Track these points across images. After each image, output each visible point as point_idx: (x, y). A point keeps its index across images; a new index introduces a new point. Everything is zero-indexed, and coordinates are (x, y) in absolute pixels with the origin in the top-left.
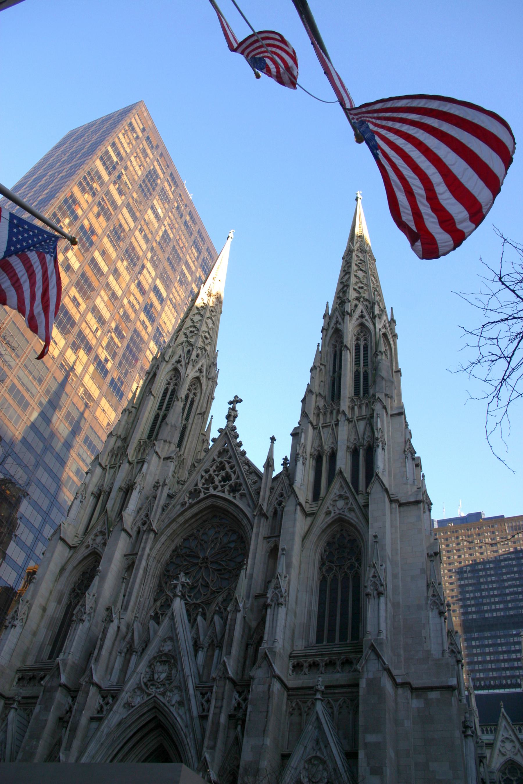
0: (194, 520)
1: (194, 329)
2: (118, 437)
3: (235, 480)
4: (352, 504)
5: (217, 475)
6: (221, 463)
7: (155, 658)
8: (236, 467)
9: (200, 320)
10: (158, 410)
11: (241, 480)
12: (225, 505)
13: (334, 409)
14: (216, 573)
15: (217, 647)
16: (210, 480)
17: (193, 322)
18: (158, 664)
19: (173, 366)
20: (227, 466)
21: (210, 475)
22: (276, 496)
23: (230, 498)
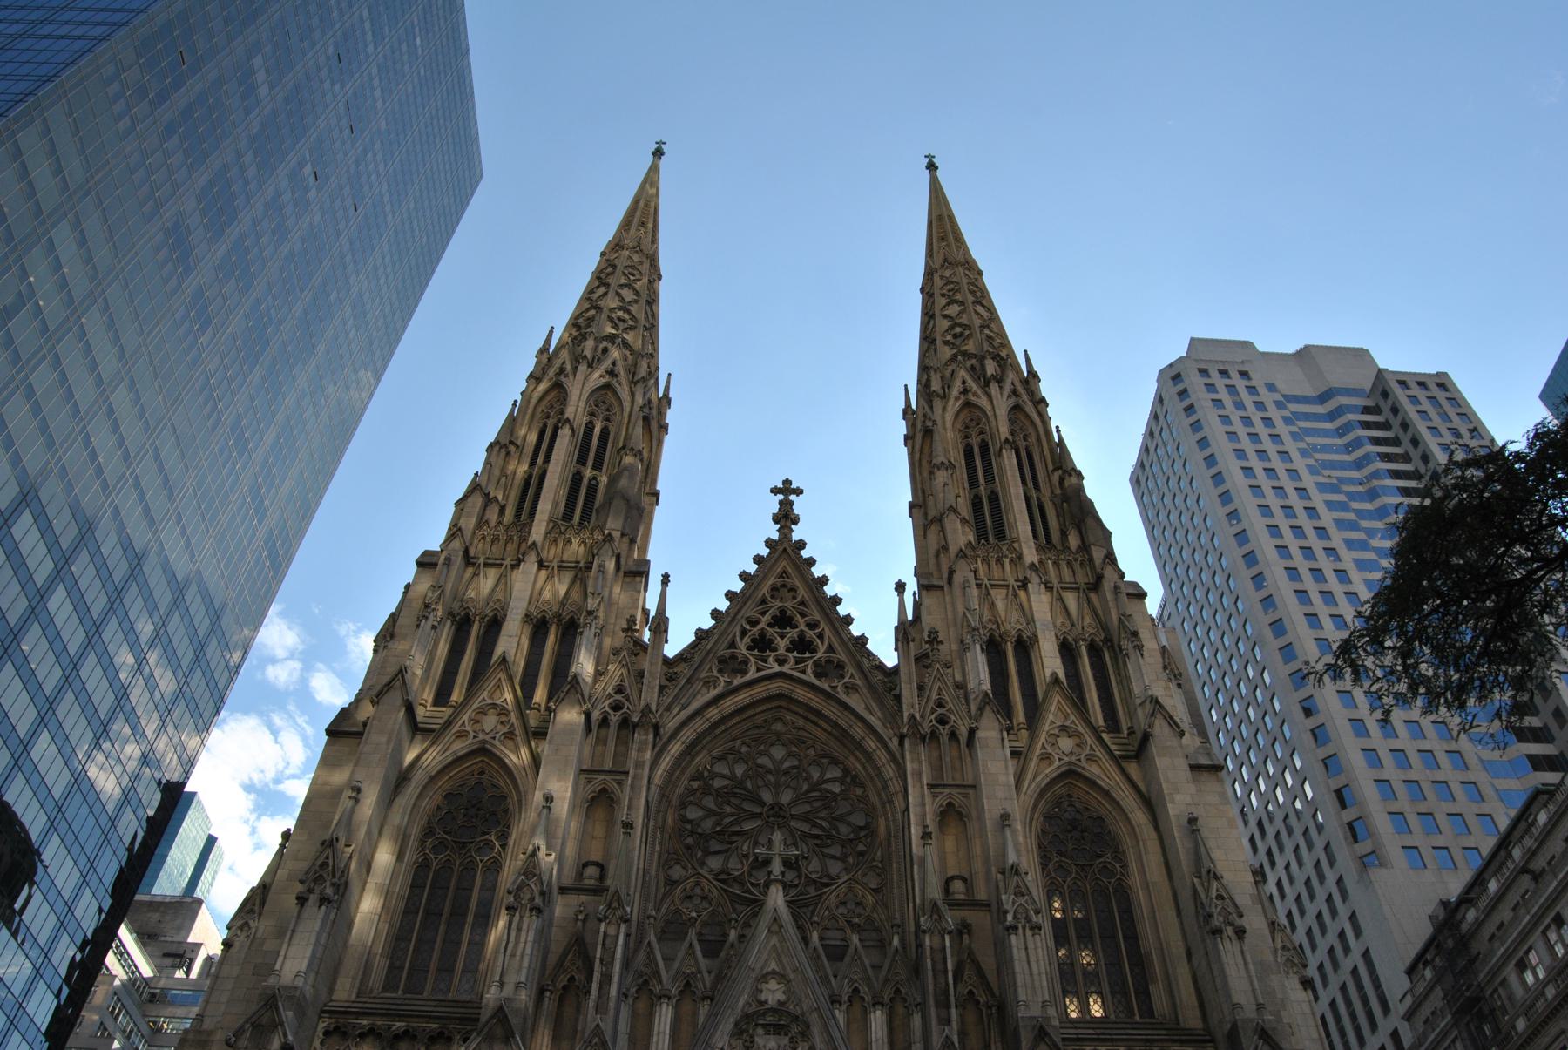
0: (736, 720)
1: (626, 316)
2: (488, 500)
3: (824, 653)
4: (1091, 746)
5: (782, 637)
6: (783, 611)
7: (747, 1017)
8: (823, 625)
9: (636, 302)
10: (578, 462)
11: (842, 656)
12: (816, 701)
13: (1006, 557)
15: (874, 1005)
17: (622, 300)
18: (760, 1031)
19: (607, 379)
20: (801, 621)
22: (931, 704)
23: (826, 687)
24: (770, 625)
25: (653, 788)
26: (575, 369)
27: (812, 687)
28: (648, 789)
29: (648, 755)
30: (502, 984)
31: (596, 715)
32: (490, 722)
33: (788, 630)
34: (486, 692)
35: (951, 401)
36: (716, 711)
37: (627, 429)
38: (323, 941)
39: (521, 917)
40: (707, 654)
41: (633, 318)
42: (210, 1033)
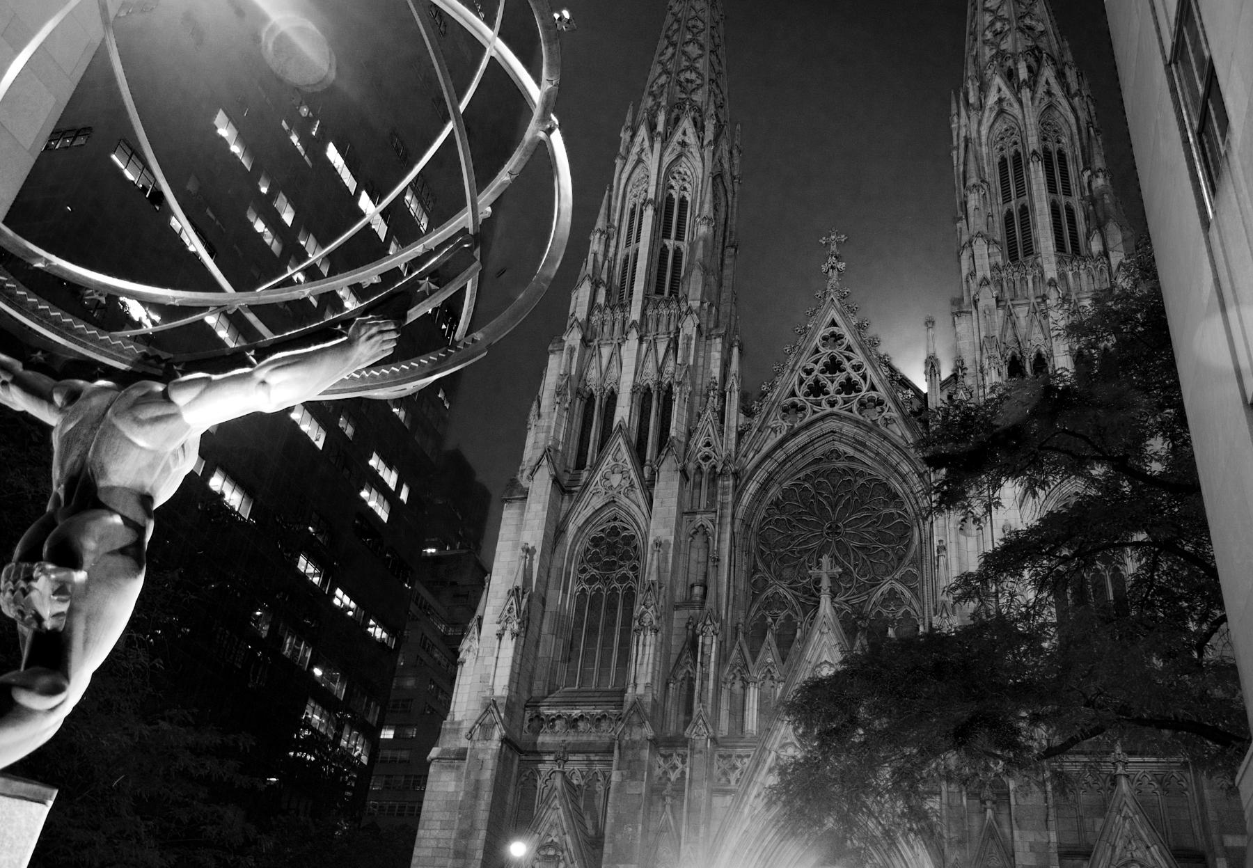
5: (833, 382)
6: (833, 358)
9: (701, 56)
14: (861, 554)
16: (817, 389)
17: (689, 59)
20: (847, 365)
21: (817, 381)
24: (823, 372)
25: (737, 522)
26: (652, 146)
27: (857, 423)
28: (733, 523)
29: (730, 498)
30: (636, 685)
31: (691, 467)
32: (616, 480)
33: (838, 373)
34: (610, 456)
35: (987, 113)
36: (782, 453)
37: (701, 196)
38: (518, 662)
39: (645, 636)
40: (773, 404)
41: (700, 75)
42: (460, 723)
